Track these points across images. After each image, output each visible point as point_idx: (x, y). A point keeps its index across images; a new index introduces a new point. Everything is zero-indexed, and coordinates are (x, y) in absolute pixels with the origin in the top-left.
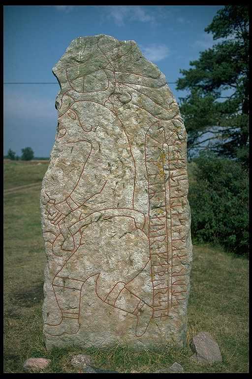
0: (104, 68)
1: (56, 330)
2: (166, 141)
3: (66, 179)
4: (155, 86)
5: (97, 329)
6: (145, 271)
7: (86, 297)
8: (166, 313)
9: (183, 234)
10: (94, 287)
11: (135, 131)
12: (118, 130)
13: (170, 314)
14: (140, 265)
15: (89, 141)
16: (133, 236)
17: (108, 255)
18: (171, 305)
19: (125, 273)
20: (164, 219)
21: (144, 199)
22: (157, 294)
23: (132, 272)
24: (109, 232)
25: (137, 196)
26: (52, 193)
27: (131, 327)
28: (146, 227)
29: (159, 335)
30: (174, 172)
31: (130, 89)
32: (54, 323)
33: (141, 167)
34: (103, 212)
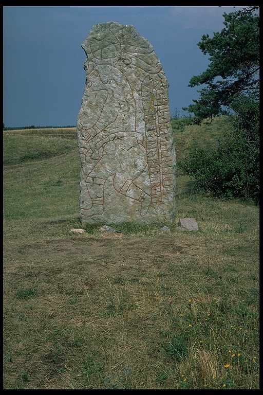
0: (113, 43)
1: (89, 213)
3: (93, 114)
5: (115, 212)
7: (107, 190)
8: (160, 200)
11: (134, 82)
13: (163, 200)
14: (141, 167)
15: (106, 90)
16: (136, 149)
18: (163, 194)
19: (132, 173)
20: (156, 137)
21: (142, 125)
22: (153, 187)
28: (145, 143)
29: (156, 214)
31: (130, 56)
32: (87, 208)
34: (117, 134)
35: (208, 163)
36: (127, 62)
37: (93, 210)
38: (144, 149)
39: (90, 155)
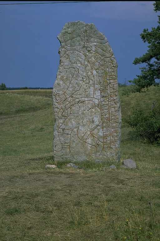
0: (80, 36)
1: (60, 154)
2: (108, 67)
4: (102, 43)
6: (100, 126)
7: (73, 138)
8: (110, 146)
9: (116, 109)
10: (76, 133)
11: (94, 63)
12: (86, 63)
13: (111, 146)
14: (97, 123)
16: (94, 110)
17: (83, 118)
21: (98, 93)
22: (105, 137)
23: (94, 126)
24: (83, 108)
25: (95, 92)
26: (58, 91)
27: (93, 152)
28: (100, 106)
30: (112, 81)
31: (92, 45)
33: (96, 79)
35: (146, 119)
36: (89, 49)
37: (63, 152)
38: (99, 110)
39: (61, 113)
